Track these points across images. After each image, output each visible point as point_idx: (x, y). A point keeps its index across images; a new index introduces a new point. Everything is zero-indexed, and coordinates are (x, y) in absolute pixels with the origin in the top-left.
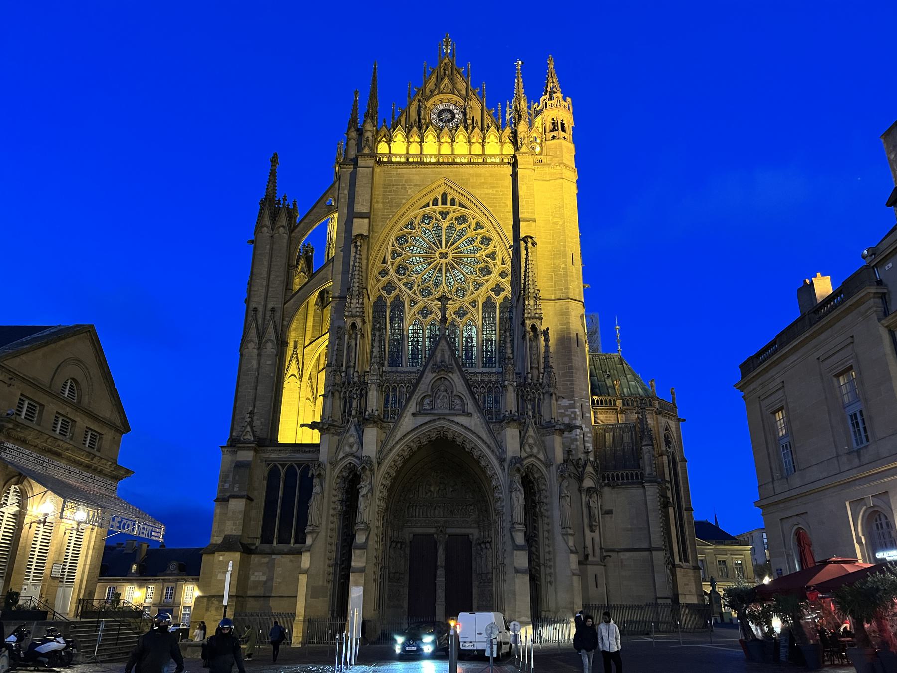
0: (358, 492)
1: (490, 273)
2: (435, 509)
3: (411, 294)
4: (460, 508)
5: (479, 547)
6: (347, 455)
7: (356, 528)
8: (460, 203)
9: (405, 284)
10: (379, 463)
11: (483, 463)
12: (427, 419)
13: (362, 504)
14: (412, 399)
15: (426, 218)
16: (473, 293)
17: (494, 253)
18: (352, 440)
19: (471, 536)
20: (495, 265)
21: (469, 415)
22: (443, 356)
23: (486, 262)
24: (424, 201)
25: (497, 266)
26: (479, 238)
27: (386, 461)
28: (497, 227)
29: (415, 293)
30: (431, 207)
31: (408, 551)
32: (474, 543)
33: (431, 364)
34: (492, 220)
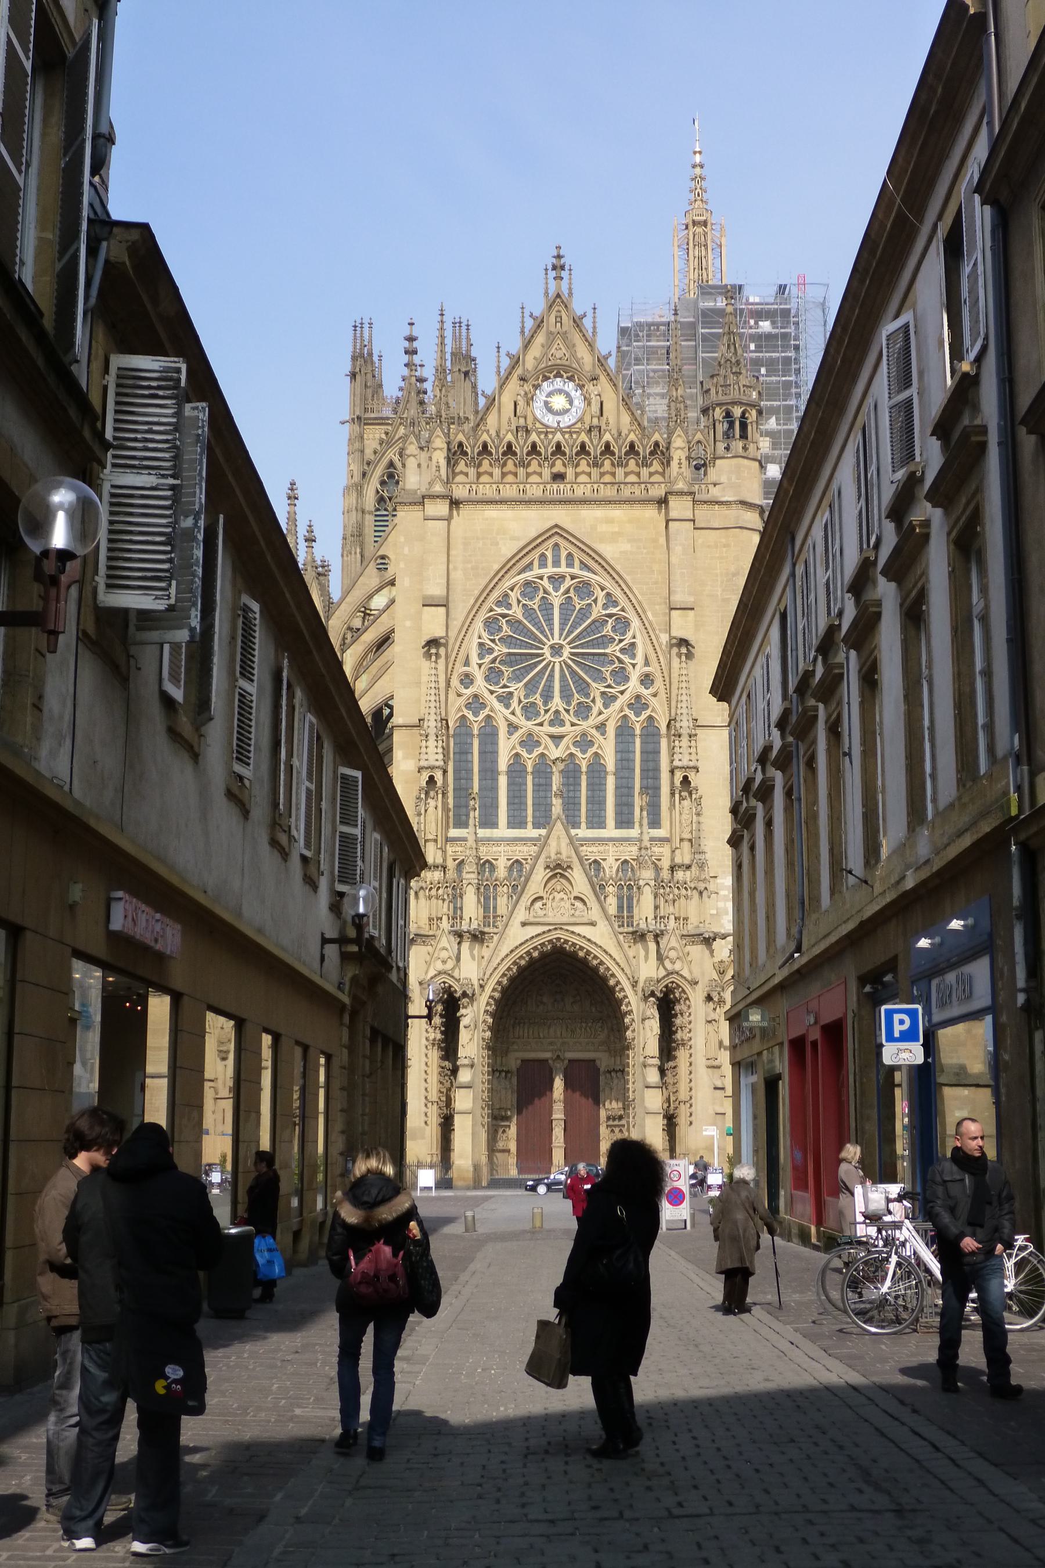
0: (457, 1021)
1: (627, 679)
2: (549, 1027)
3: (511, 718)
4: (584, 1025)
5: (608, 1075)
6: (440, 973)
7: (458, 1063)
8: (581, 562)
9: (500, 699)
10: (481, 986)
11: (612, 982)
12: (539, 929)
13: (464, 1036)
14: (520, 902)
15: (530, 588)
16: (600, 713)
17: (633, 645)
18: (444, 954)
19: (598, 1062)
20: (634, 665)
21: (593, 924)
22: (559, 845)
23: (620, 661)
24: (526, 561)
25: (638, 667)
26: (610, 621)
27: (490, 981)
28: (637, 607)
29: (513, 713)
30: (537, 571)
31: (515, 1080)
32: (602, 1070)
33: (543, 856)
34: (630, 595)
